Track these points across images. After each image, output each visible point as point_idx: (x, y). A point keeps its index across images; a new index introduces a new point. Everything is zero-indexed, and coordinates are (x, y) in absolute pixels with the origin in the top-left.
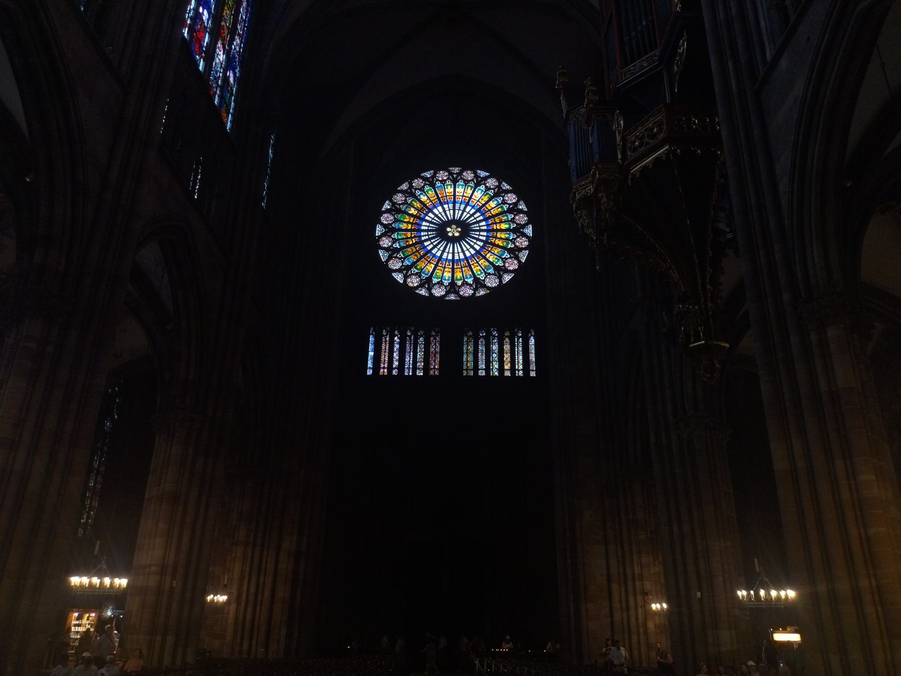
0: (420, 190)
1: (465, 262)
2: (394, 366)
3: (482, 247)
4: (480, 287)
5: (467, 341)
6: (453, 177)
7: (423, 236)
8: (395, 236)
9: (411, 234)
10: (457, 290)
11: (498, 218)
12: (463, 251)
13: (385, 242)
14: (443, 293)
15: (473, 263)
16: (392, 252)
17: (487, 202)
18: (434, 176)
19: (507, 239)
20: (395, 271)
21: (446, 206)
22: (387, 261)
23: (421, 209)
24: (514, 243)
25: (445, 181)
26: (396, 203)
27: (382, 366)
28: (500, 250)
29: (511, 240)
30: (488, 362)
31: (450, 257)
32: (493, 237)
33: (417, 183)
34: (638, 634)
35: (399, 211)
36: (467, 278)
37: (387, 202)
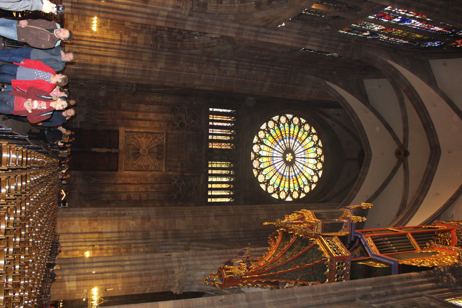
1: (272, 164)
2: (214, 123)
3: (280, 173)
4: (258, 172)
5: (228, 164)
6: (319, 157)
8: (286, 125)
12: (278, 162)
13: (283, 119)
14: (255, 151)
16: (278, 123)
17: (305, 176)
18: (319, 147)
19: (284, 187)
21: (303, 153)
22: (273, 120)
25: (317, 153)
27: (214, 116)
30: (216, 175)
31: (275, 155)
32: (286, 179)
33: (315, 138)
34: (73, 246)
35: (300, 128)
37: (305, 121)
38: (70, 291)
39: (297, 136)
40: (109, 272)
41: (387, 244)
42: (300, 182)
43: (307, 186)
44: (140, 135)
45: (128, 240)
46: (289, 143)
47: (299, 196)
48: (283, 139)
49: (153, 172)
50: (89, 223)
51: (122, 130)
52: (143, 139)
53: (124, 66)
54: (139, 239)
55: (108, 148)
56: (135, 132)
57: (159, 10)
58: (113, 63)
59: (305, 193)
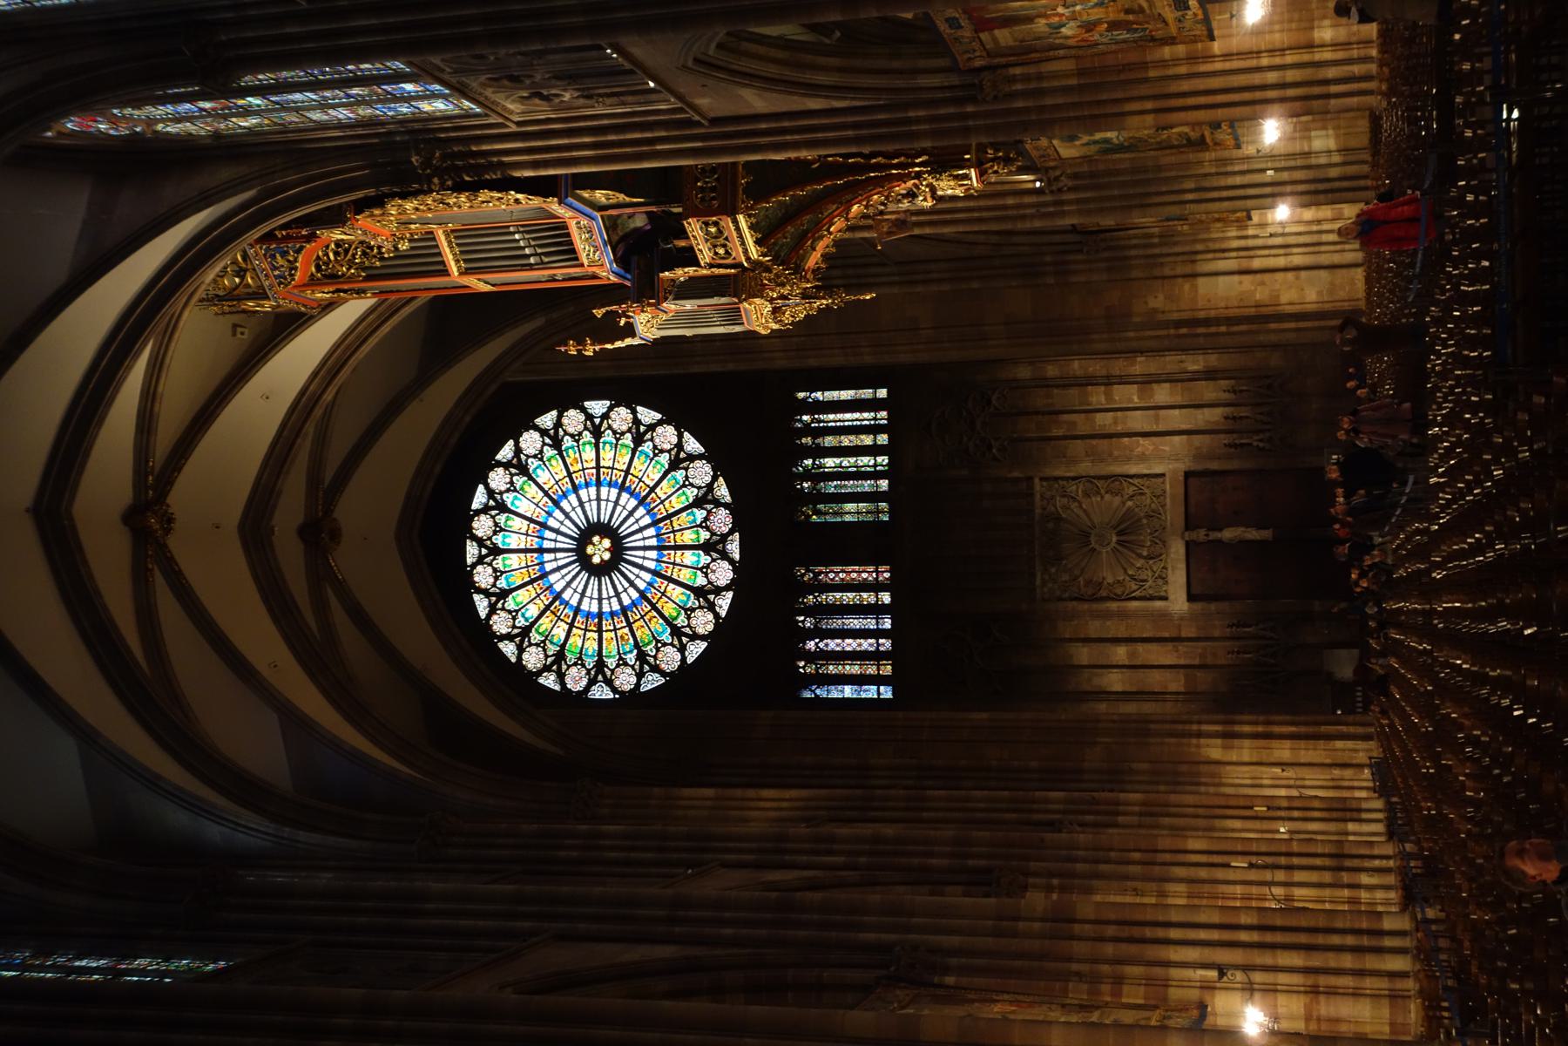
0: (514, 618)
1: (661, 525)
3: (632, 494)
9: (606, 631)
12: (641, 530)
13: (626, 680)
14: (726, 565)
15: (663, 510)
18: (486, 593)
20: (684, 659)
21: (548, 567)
22: (663, 673)
24: (623, 434)
25: (495, 570)
28: (636, 459)
29: (618, 440)
30: (860, 475)
31: (653, 554)
33: (500, 624)
35: (560, 656)
36: (694, 521)
37: (541, 680)
38: (1325, 128)
39: (571, 625)
40: (1235, 173)
41: (534, 246)
42: (558, 467)
43: (532, 451)
44: (1119, 591)
45: (1169, 255)
47: (560, 416)
48: (624, 610)
50: (1278, 296)
51: (1178, 602)
52: (1110, 580)
53: (1202, 741)
54: (1136, 257)
55: (1220, 541)
56: (1135, 599)
57: (1140, 826)
58: (1232, 747)
59: (536, 428)
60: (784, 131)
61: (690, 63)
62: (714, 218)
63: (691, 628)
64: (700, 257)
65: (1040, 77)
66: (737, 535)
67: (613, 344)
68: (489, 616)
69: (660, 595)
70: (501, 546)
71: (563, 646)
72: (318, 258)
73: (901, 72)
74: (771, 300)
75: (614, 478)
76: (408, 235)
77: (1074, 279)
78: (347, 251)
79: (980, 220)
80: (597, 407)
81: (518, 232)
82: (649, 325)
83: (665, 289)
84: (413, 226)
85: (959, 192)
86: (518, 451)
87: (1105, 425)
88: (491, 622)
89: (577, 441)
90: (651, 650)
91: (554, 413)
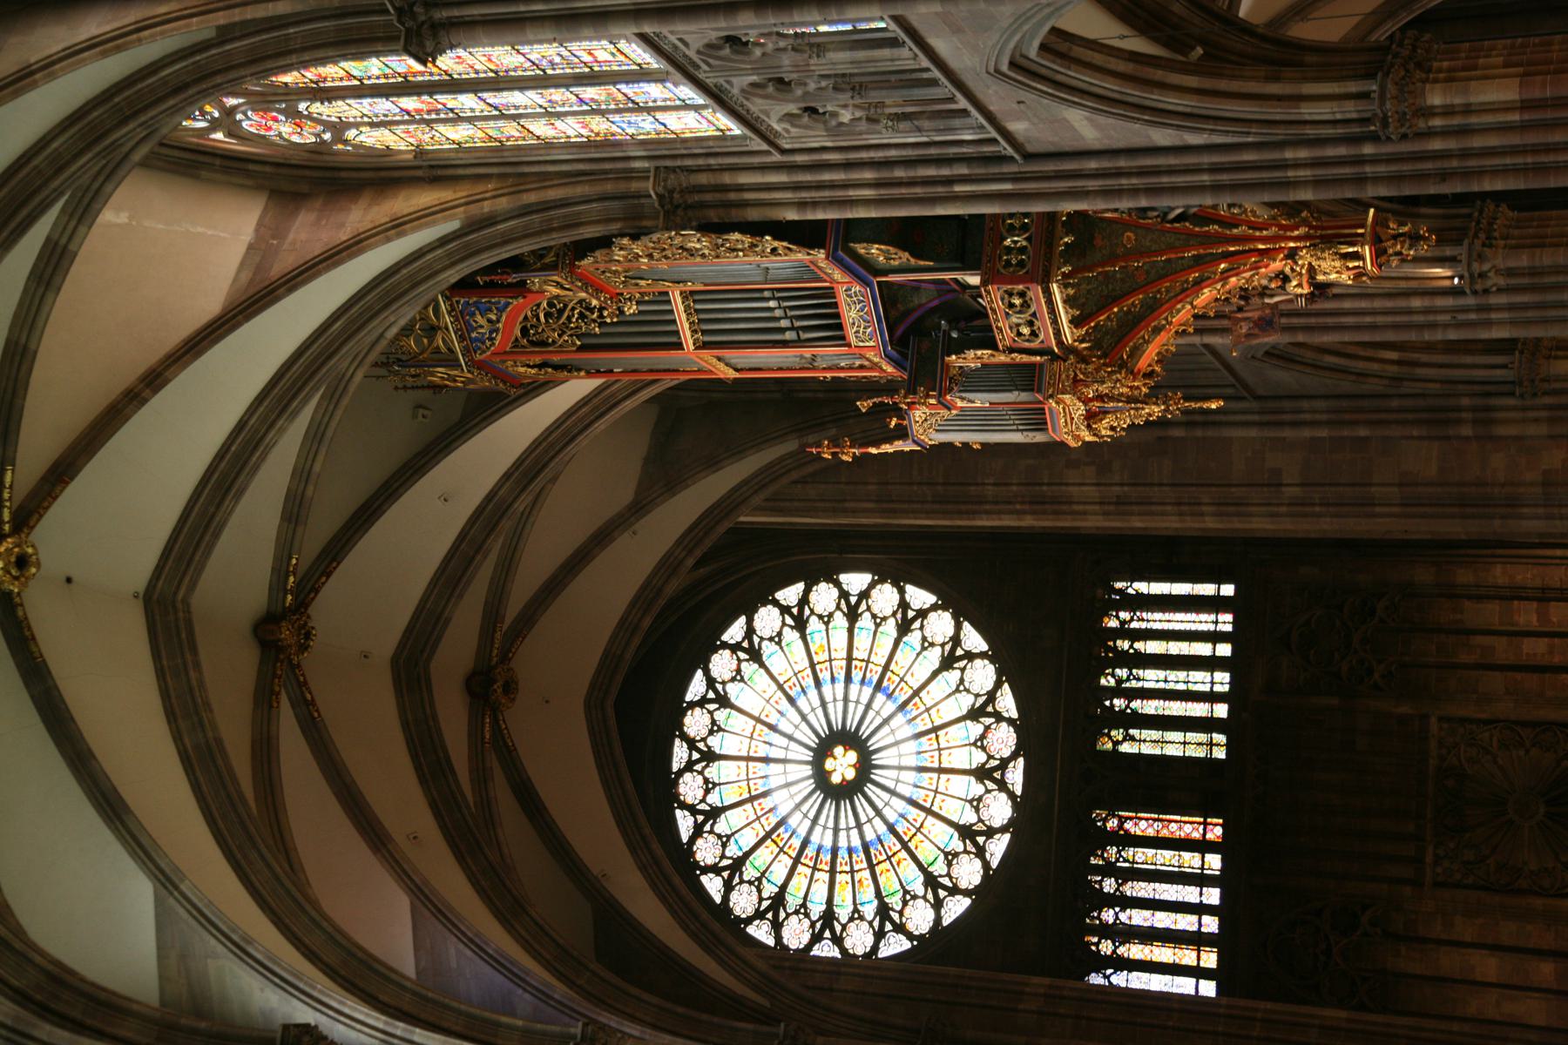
0: (724, 846)
3: (890, 696)
6: (698, 761)
7: (849, 841)
8: (843, 913)
9: (840, 872)
10: (998, 762)
11: (816, 653)
18: (692, 810)
22: (910, 936)
23: (778, 846)
24: (884, 619)
25: (706, 781)
26: (757, 910)
33: (706, 852)
35: (779, 900)
37: (751, 930)
39: (797, 861)
41: (791, 318)
46: (836, 830)
47: (807, 592)
49: (1483, 716)
59: (776, 603)
60: (1119, 173)
61: (1005, 68)
62: (1021, 287)
63: (951, 878)
64: (998, 337)
65: (1468, 110)
66: (1021, 761)
67: (878, 448)
68: (693, 840)
69: (914, 830)
70: (718, 752)
71: (783, 888)
72: (526, 318)
73: (1279, 98)
74: (1086, 401)
75: (868, 675)
76: (638, 295)
77: (1502, 431)
78: (561, 312)
79: (1373, 327)
80: (855, 581)
81: (773, 298)
82: (925, 425)
83: (951, 379)
84: (642, 283)
85: (1346, 278)
86: (750, 631)
87: (1535, 654)
88: (695, 848)
89: (827, 624)
90: (896, 903)
91: (801, 586)
